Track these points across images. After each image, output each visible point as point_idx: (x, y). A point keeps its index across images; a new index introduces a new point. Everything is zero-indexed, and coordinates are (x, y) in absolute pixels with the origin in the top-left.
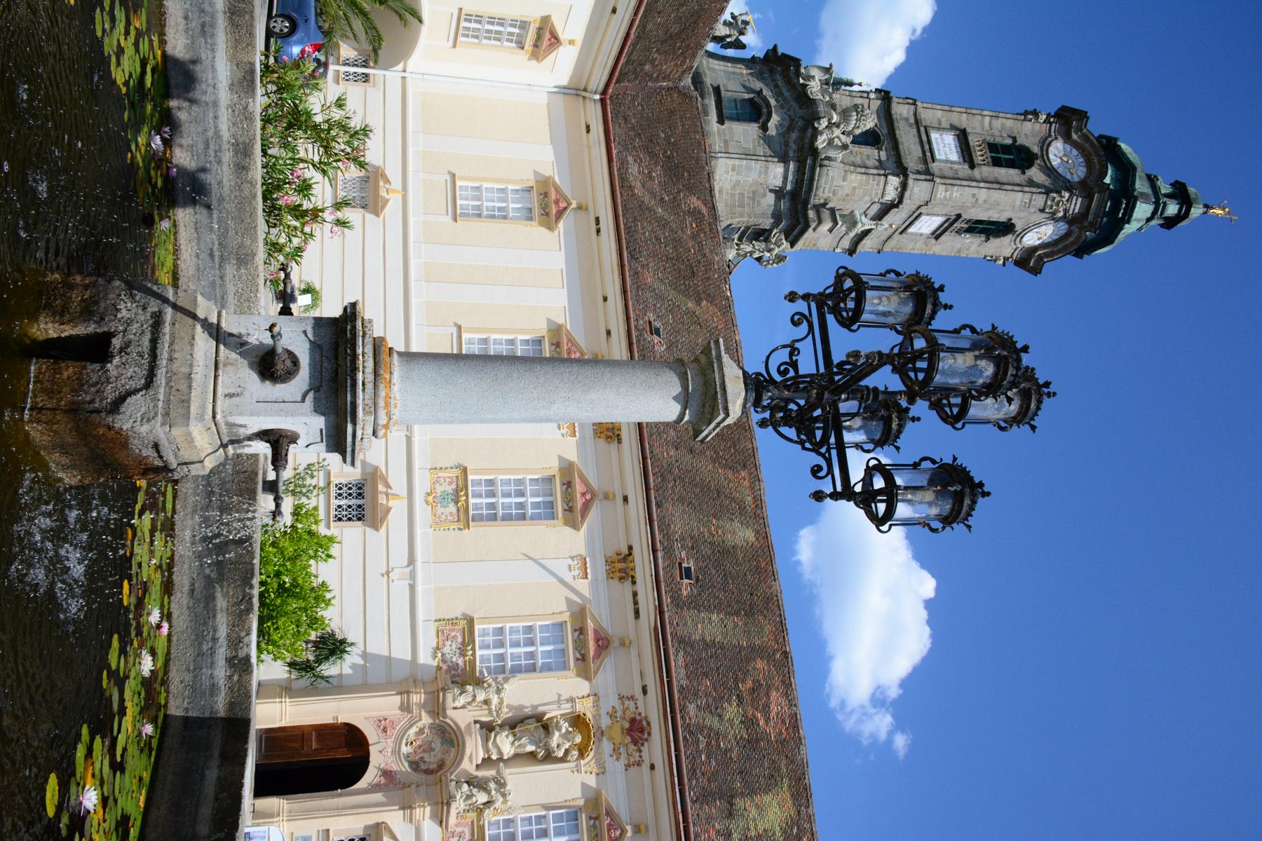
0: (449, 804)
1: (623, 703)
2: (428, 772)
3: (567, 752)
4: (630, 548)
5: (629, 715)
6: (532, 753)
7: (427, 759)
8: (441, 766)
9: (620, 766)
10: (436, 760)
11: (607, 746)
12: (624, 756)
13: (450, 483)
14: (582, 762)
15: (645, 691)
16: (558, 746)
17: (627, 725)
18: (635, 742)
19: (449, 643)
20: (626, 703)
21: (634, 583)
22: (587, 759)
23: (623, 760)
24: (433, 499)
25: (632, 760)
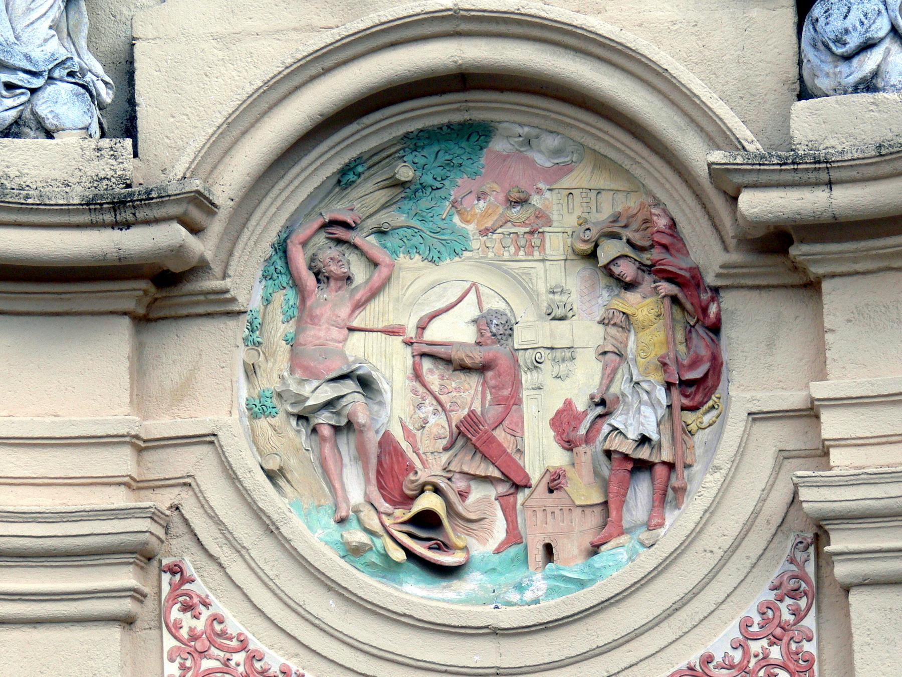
7: (581, 383)
8: (640, 260)
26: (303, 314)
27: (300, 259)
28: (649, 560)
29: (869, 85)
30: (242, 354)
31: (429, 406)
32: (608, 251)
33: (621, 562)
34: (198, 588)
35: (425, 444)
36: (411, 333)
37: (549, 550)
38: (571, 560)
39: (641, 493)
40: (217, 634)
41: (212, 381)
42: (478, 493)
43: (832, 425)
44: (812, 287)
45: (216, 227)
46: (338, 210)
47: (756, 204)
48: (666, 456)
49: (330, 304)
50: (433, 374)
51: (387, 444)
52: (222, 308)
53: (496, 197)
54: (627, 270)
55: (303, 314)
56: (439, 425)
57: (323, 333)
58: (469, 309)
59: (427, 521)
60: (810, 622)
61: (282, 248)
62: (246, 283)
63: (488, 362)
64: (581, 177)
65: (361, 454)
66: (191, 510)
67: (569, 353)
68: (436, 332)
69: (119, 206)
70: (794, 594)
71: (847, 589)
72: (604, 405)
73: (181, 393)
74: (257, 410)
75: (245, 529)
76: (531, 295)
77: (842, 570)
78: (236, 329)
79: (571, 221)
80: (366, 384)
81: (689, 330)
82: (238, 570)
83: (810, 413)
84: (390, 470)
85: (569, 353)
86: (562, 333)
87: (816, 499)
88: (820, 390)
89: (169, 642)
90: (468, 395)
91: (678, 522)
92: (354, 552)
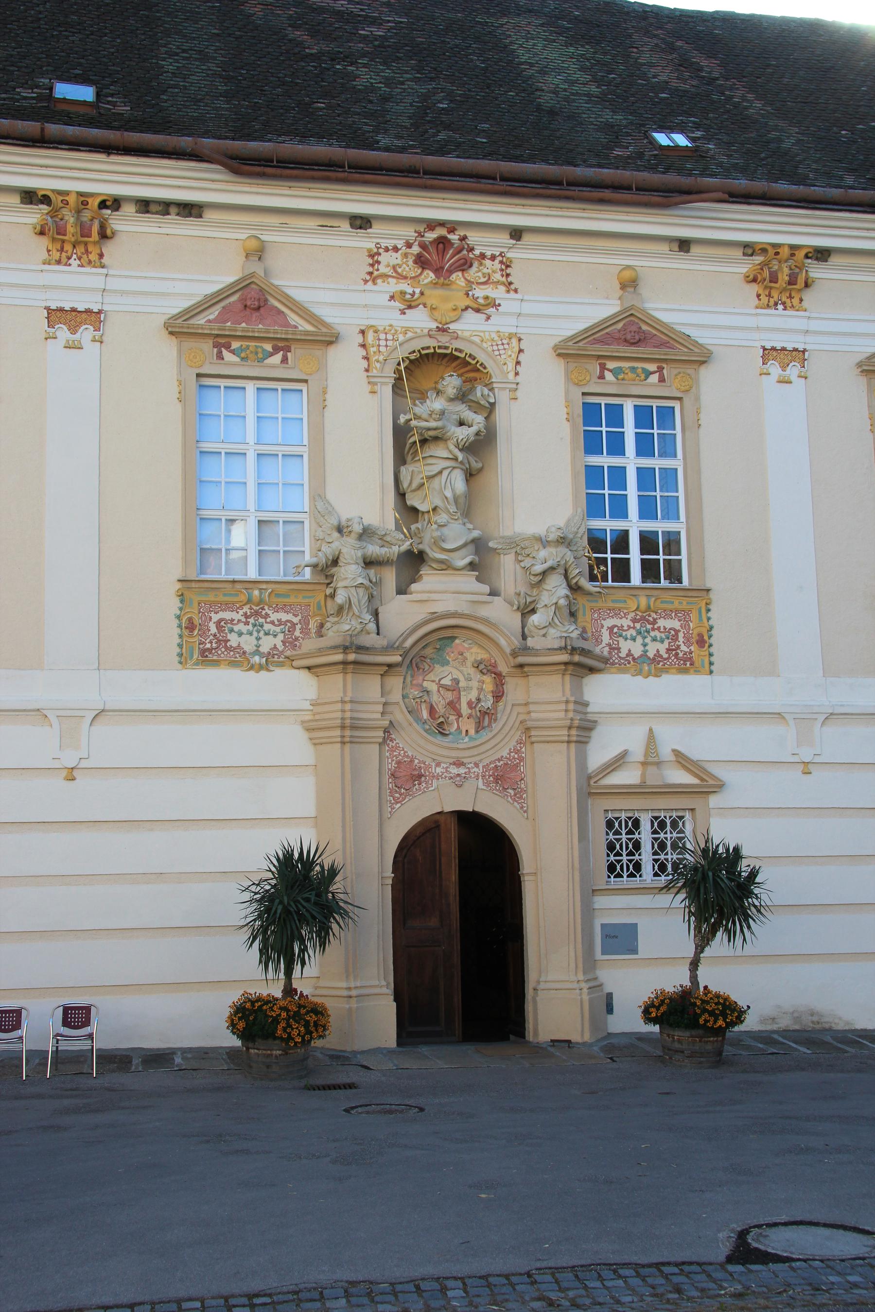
1: (385, 276)
2: (498, 696)
3: (476, 407)
4: (29, 197)
5: (409, 268)
7: (473, 696)
9: (508, 303)
10: (477, 676)
15: (361, 222)
17: (429, 276)
18: (465, 265)
19: (234, 640)
20: (383, 269)
21: (114, 203)
23: (498, 293)
25: (497, 277)
28: (491, 735)
31: (441, 699)
35: (440, 707)
36: (437, 680)
37: (467, 731)
40: (397, 747)
48: (492, 712)
50: (442, 691)
53: (456, 652)
56: (443, 702)
58: (450, 677)
60: (523, 750)
61: (411, 661)
67: (471, 688)
68: (442, 682)
70: (521, 743)
71: (532, 743)
72: (479, 700)
76: (464, 675)
77: (533, 739)
79: (472, 659)
81: (497, 685)
85: (471, 688)
87: (530, 724)
89: (387, 748)
90: (449, 696)
91: (496, 727)
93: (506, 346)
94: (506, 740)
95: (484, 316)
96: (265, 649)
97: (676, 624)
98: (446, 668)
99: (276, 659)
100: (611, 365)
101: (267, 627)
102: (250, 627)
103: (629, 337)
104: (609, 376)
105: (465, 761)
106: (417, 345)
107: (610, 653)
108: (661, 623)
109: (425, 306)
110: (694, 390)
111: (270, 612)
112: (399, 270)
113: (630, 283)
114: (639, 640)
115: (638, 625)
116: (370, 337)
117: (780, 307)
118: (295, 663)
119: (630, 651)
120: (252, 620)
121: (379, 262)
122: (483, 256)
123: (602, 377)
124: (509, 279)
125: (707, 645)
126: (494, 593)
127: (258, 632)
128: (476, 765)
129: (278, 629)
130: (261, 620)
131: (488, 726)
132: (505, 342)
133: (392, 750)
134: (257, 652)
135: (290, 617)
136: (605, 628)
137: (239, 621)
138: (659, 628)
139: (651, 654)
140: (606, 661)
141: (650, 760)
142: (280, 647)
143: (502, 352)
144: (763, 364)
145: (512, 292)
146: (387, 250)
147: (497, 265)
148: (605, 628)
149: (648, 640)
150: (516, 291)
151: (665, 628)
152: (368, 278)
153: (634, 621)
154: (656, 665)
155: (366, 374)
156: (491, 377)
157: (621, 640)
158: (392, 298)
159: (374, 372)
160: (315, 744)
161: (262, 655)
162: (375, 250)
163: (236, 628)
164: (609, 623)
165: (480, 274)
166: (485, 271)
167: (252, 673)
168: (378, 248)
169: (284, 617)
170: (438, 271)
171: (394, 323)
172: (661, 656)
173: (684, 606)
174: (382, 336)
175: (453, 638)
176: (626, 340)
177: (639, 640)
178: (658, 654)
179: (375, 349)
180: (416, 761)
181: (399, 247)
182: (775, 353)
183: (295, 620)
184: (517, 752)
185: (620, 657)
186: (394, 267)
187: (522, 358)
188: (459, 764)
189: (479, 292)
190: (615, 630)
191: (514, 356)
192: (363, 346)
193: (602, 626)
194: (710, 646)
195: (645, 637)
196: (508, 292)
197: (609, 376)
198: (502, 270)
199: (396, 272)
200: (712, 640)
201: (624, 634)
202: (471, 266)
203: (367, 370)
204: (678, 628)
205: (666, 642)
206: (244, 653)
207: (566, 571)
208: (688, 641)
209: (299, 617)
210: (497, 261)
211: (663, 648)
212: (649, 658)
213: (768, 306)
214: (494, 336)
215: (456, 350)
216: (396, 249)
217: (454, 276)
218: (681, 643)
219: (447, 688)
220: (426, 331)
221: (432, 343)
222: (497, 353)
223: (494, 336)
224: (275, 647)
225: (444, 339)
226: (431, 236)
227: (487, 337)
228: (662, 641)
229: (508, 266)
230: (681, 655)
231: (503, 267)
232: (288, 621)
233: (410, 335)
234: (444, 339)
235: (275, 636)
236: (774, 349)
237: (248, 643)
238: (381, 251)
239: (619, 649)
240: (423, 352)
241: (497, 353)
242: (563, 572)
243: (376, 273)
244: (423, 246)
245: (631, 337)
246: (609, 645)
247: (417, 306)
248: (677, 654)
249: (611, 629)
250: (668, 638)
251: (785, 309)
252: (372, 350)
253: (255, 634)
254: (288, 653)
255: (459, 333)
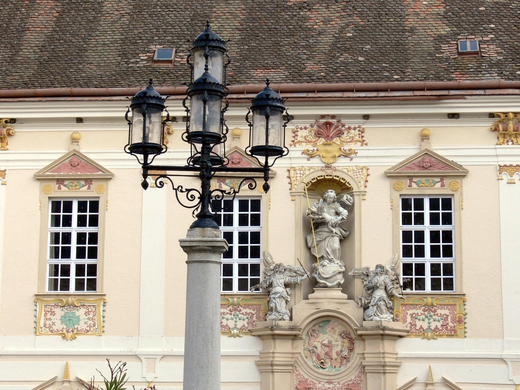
0: (384, 329)
3: (344, 205)
6: (341, 241)
7: (339, 349)
8: (346, 336)
10: (340, 340)
11: (342, 163)
12: (352, 146)
13: (53, 313)
14: (355, 189)
16: (337, 214)
17: (322, 140)
18: (340, 134)
20: (299, 139)
22: (353, 185)
24: (70, 333)
25: (357, 138)
26: (309, 340)
27: (309, 333)
28: (346, 368)
29: (371, 320)
30: (303, 344)
32: (343, 335)
33: (343, 368)
34: (298, 369)
38: (337, 368)
39: (345, 360)
41: (300, 347)
42: (328, 360)
43: (366, 356)
44: (364, 340)
45: (302, 331)
46: (314, 328)
47: (359, 332)
49: (313, 339)
50: (323, 347)
51: (318, 354)
52: (301, 339)
53: (331, 328)
54: (344, 337)
55: (309, 340)
56: (323, 352)
57: (311, 342)
58: (327, 340)
59: (322, 363)
61: (308, 332)
62: (304, 336)
63: (329, 346)
64: (340, 326)
65: (315, 355)
66: (297, 360)
67: (338, 345)
68: (324, 342)
69: (292, 329)
72: (341, 351)
73: (297, 348)
74: (304, 350)
75: (302, 362)
77: (366, 371)
78: (302, 341)
80: (316, 347)
82: (302, 367)
83: (364, 354)
84: (318, 357)
85: (338, 345)
86: (337, 343)
87: (364, 364)
88: (365, 352)
90: (327, 349)
91: (349, 365)
92: (314, 366)
93: (361, 173)
94: (353, 372)
95: (349, 159)
96: (239, 326)
97: (447, 312)
98: (325, 335)
99: (244, 331)
100: (415, 180)
101: (240, 316)
102: (232, 316)
103: (424, 165)
104: (414, 185)
105: (333, 381)
106: (316, 175)
107: (411, 327)
108: (439, 311)
109: (319, 156)
110: (460, 190)
111: (242, 309)
112: (307, 139)
113: (425, 137)
114: (427, 320)
115: (426, 313)
116: (292, 173)
117: (510, 143)
118: (252, 333)
119: (421, 326)
120: (233, 313)
121: (297, 135)
122: (349, 128)
123: (410, 186)
124: (363, 139)
125: (463, 323)
126: (350, 298)
127: (236, 318)
128: (339, 383)
129: (245, 317)
130: (238, 313)
131: (346, 364)
132: (360, 171)
133: (297, 375)
134: (235, 327)
135: (251, 311)
136: (409, 314)
137: (227, 313)
138: (438, 314)
139: (433, 328)
140: (408, 332)
141: (429, 382)
142: (246, 325)
143: (359, 176)
144: (500, 174)
145: (364, 145)
146: (301, 129)
147: (357, 132)
148: (409, 314)
149: (431, 320)
150: (366, 144)
151: (441, 314)
152: (292, 143)
153: (424, 310)
154: (436, 333)
155: (290, 191)
156: (353, 189)
157: (417, 320)
158: (303, 153)
159: (294, 190)
160: (261, 372)
161: (238, 329)
162: (296, 130)
163: (226, 317)
164: (410, 312)
165: (348, 137)
166: (351, 135)
167: (232, 338)
168: (297, 128)
169: (248, 311)
170: (327, 137)
171: (304, 165)
172: (438, 329)
173: (451, 302)
174: (298, 172)
175: (329, 321)
176: (423, 167)
177: (427, 320)
178: (437, 328)
179: (294, 179)
180: (309, 381)
181: (307, 127)
182: (506, 168)
183: (254, 312)
184: (359, 377)
185: (417, 330)
186: (305, 137)
187: (369, 178)
188: (330, 382)
189: (347, 147)
190: (414, 315)
191: (364, 178)
192: (289, 177)
193: (407, 314)
194: (465, 323)
195: (429, 319)
196: (362, 145)
197: (414, 185)
198: (359, 134)
199: (306, 139)
200: (466, 321)
201: (418, 317)
202: (343, 134)
203: (290, 189)
204: (448, 314)
205: (441, 321)
206: (229, 328)
207: (386, 287)
208: (453, 320)
209: (256, 311)
210: (357, 130)
211: (439, 325)
212: (431, 330)
213: (503, 143)
214: (354, 168)
215: (335, 176)
216: (306, 128)
217: (335, 139)
218: (449, 322)
219: (325, 346)
220: (320, 168)
221: (323, 173)
222: (356, 177)
223: (354, 168)
224: (244, 325)
225: (329, 172)
226: (323, 121)
227: (351, 169)
228: (439, 321)
229: (362, 132)
230: (449, 328)
231: (360, 133)
232: (250, 313)
233: (312, 170)
234: (329, 172)
235: (244, 320)
236: (505, 166)
237: (231, 324)
238: (298, 129)
239: (415, 325)
240: (319, 178)
241: (356, 177)
242: (383, 288)
243: (296, 141)
244: (319, 127)
245: (427, 164)
246: (411, 323)
247: (315, 156)
248: (447, 327)
249: (412, 315)
250: (442, 319)
251: (513, 144)
252: (293, 179)
253: (235, 319)
254: (250, 328)
255: (337, 168)
